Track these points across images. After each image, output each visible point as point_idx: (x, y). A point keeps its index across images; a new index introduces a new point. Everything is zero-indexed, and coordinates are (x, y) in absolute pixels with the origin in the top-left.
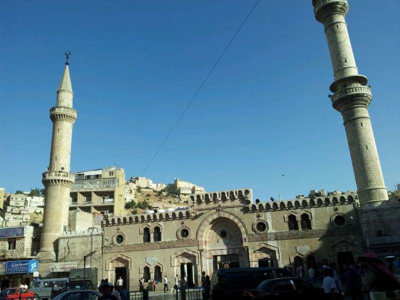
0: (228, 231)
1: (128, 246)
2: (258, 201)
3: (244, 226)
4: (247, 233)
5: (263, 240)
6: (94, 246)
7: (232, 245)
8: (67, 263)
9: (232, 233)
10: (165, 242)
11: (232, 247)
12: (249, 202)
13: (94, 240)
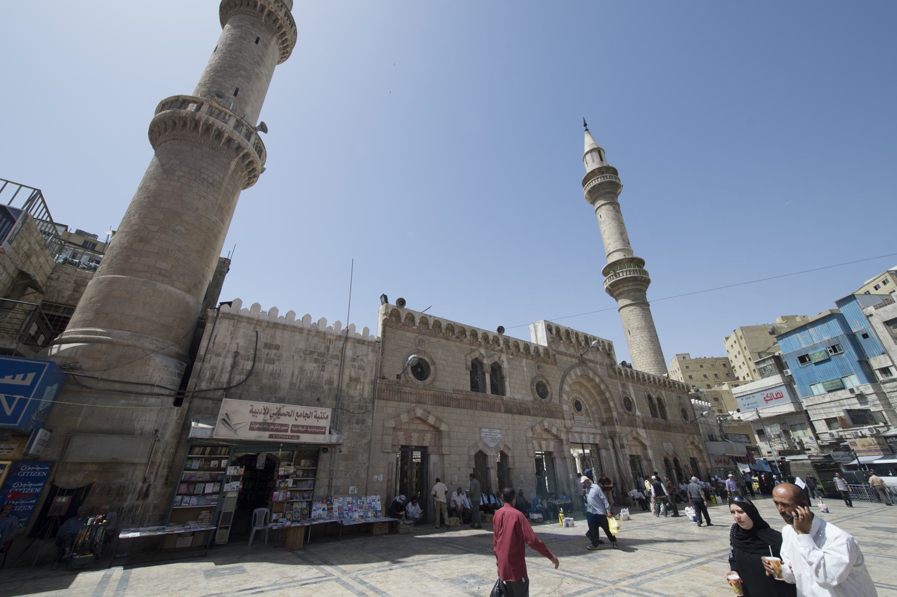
3: (613, 400)
4: (617, 411)
8: (288, 408)
12: (615, 363)
13: (349, 353)
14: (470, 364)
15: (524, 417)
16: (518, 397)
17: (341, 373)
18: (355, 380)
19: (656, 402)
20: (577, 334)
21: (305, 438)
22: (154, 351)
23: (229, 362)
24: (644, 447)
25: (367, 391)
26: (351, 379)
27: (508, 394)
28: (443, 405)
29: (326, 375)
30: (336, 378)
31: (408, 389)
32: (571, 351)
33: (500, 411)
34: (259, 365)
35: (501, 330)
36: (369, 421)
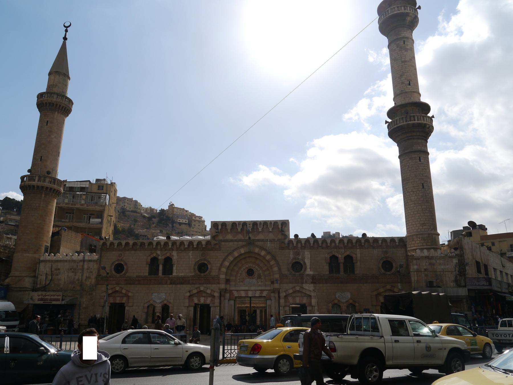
2: (296, 236)
6: (86, 274)
7: (260, 286)
8: (48, 293)
9: (261, 272)
11: (260, 288)
13: (86, 266)
14: (149, 260)
15: (184, 286)
16: (181, 275)
17: (82, 275)
18: (88, 278)
21: (54, 303)
22: (26, 276)
23: (44, 277)
24: (310, 296)
25: (93, 281)
26: (87, 277)
27: (174, 274)
28: (131, 284)
29: (77, 277)
30: (80, 277)
31: (111, 279)
32: (240, 237)
33: (166, 284)
34: (54, 277)
36: (94, 294)
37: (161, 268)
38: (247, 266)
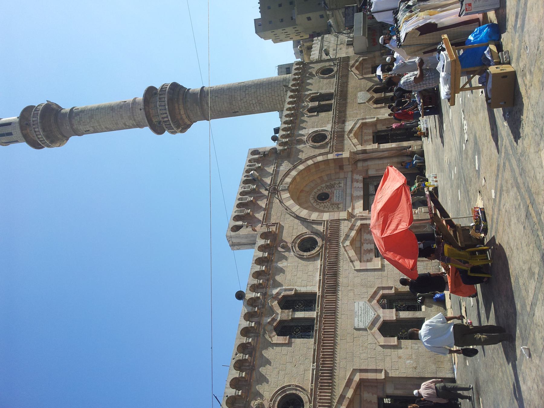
0: (319, 190)
1: (317, 378)
3: (315, 156)
5: (343, 136)
9: (324, 185)
10: (323, 282)
11: (349, 183)
12: (274, 150)
19: (316, 104)
20: (242, 194)
33: (335, 302)
35: (240, 296)
37: (299, 315)
38: (312, 201)
